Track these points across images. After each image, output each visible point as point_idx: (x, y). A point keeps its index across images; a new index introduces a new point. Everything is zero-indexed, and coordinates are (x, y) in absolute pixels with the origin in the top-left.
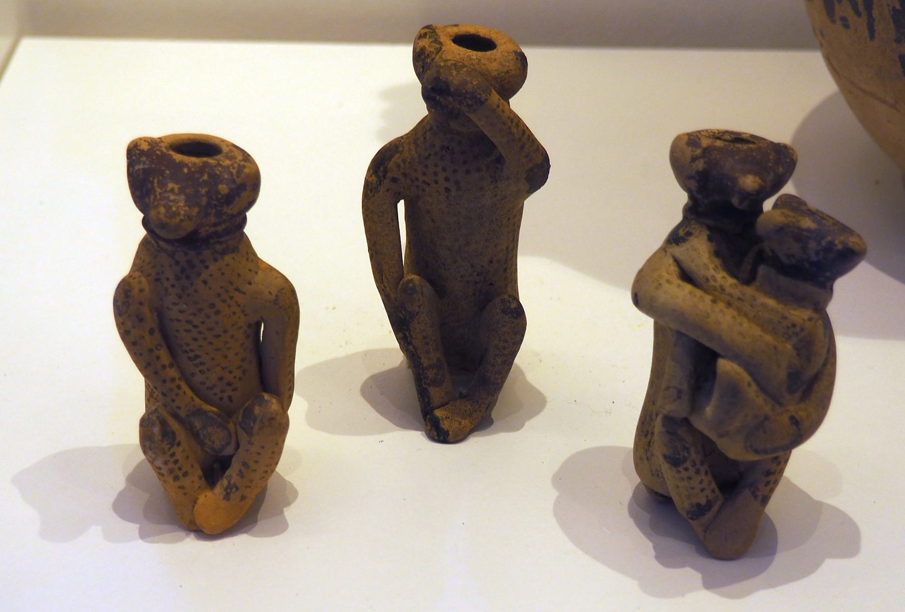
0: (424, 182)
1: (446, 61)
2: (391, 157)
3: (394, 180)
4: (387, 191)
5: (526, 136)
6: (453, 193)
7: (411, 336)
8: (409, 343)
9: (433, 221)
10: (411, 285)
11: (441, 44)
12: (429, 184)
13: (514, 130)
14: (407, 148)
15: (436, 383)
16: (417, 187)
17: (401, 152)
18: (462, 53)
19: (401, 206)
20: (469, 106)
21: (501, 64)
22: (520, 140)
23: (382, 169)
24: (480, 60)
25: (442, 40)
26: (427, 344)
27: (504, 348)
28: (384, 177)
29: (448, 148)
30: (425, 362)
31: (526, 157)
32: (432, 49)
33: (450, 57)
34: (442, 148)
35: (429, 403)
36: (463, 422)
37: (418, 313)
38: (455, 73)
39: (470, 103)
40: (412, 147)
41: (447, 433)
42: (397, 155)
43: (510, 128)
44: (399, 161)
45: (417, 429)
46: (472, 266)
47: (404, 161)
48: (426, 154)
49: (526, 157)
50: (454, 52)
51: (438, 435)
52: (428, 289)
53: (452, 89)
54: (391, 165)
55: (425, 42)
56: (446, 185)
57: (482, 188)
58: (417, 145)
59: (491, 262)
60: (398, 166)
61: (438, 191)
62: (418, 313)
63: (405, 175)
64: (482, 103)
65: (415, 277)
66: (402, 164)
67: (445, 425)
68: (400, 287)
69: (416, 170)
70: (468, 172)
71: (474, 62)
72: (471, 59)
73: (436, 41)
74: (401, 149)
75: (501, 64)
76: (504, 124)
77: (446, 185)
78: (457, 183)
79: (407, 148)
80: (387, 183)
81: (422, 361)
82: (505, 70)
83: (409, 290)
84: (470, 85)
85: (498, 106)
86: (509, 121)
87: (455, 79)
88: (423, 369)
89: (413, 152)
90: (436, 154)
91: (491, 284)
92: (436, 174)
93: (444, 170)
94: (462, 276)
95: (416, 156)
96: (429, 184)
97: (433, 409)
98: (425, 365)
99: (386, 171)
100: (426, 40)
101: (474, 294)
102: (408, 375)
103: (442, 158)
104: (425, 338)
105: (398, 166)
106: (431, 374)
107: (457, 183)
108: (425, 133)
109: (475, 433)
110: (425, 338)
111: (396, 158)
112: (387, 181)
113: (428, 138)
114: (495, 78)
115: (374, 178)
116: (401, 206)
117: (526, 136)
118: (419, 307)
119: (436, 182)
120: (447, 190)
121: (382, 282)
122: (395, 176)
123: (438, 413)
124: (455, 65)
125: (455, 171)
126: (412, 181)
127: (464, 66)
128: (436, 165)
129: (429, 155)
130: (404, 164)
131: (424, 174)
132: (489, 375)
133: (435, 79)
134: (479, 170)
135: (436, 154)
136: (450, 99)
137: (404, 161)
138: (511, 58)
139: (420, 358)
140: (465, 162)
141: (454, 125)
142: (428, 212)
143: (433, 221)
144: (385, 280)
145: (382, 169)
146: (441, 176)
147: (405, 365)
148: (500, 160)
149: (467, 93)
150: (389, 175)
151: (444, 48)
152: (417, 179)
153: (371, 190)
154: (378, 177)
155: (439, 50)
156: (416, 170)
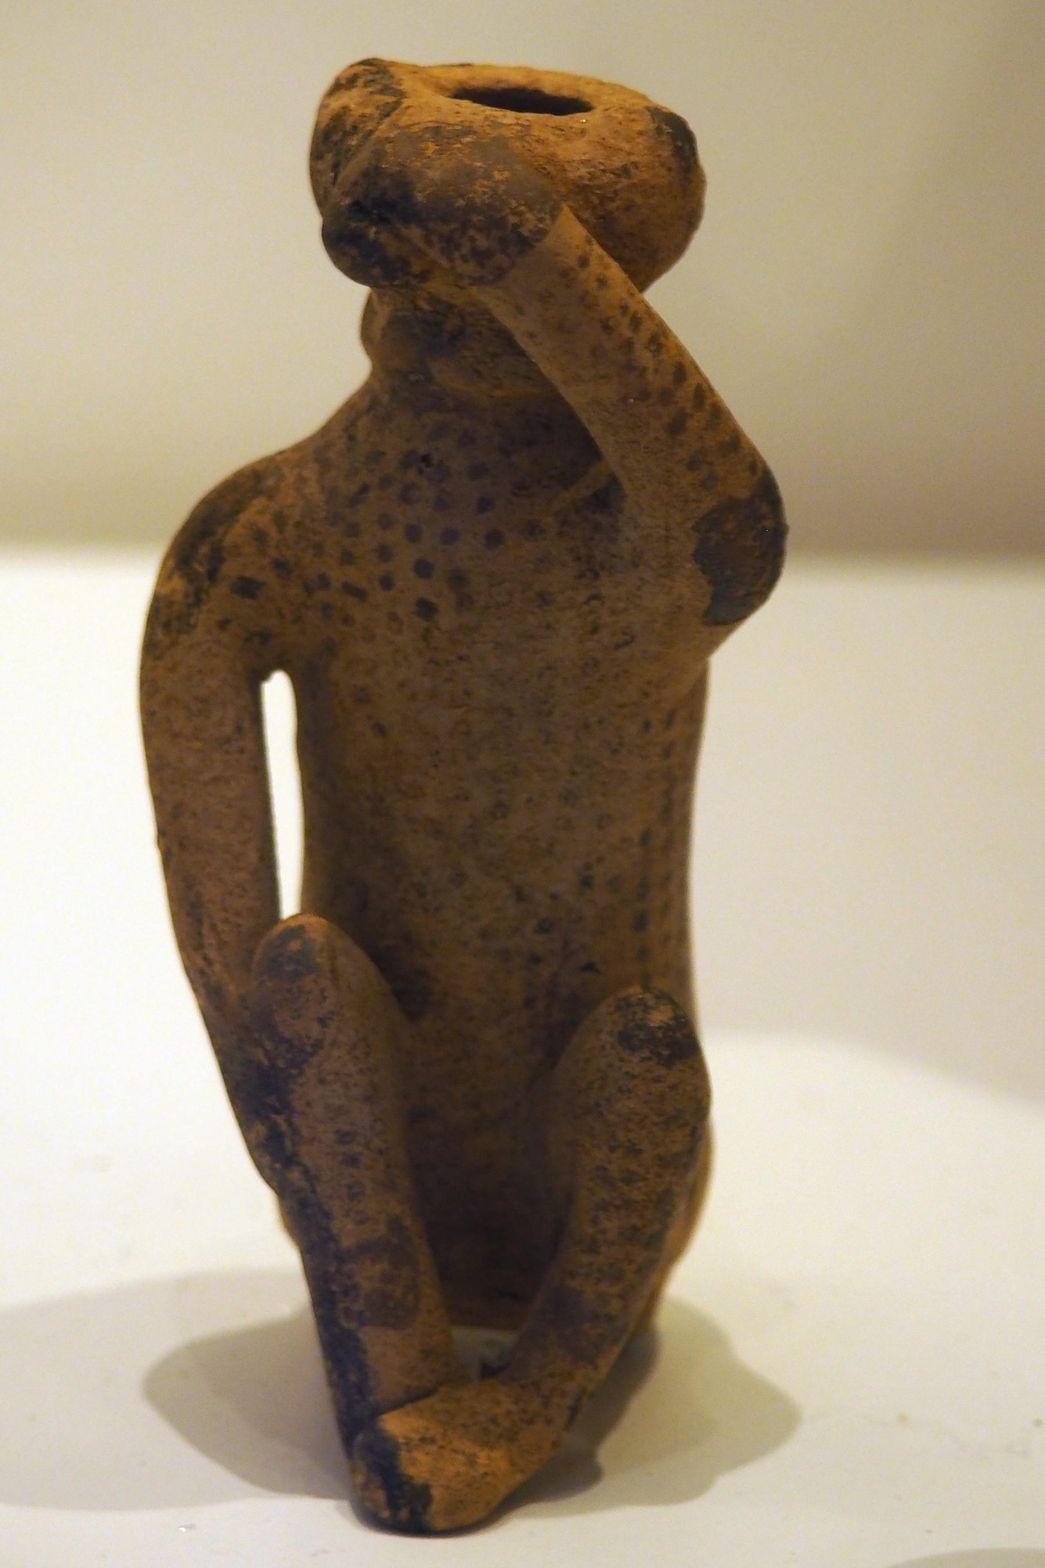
0: (349, 589)
2: (239, 507)
3: (247, 588)
4: (223, 625)
6: (447, 619)
7: (295, 1132)
9: (381, 730)
10: (295, 946)
12: (360, 594)
13: (645, 357)
14: (290, 476)
15: (390, 1312)
16: (327, 609)
17: (271, 494)
19: (278, 695)
20: (481, 256)
22: (666, 397)
23: (204, 549)
26: (353, 1161)
27: (629, 1178)
28: (212, 575)
29: (426, 459)
30: (348, 1232)
31: (693, 465)
34: (408, 460)
35: (362, 1389)
36: (483, 1456)
37: (318, 1045)
39: (482, 243)
40: (310, 472)
41: (422, 1495)
42: (259, 503)
43: (628, 346)
44: (264, 522)
46: (520, 896)
48: (354, 488)
49: (693, 465)
51: (393, 1503)
52: (356, 965)
53: (420, 197)
54: (236, 534)
56: (423, 589)
59: (586, 883)
60: (260, 537)
61: (393, 617)
62: (318, 1045)
63: (280, 565)
64: (524, 244)
66: (273, 533)
67: (417, 1466)
69: (318, 549)
70: (494, 539)
76: (607, 328)
77: (423, 589)
78: (458, 580)
79: (290, 476)
80: (220, 599)
81: (336, 1226)
82: (618, 162)
86: (626, 321)
88: (341, 1258)
89: (312, 489)
92: (384, 553)
94: (484, 934)
96: (360, 594)
97: (377, 1412)
98: (347, 1242)
99: (217, 558)
101: (529, 1003)
103: (405, 497)
104: (344, 1137)
106: (367, 1276)
107: (458, 580)
109: (532, 1508)
110: (344, 1137)
112: (220, 591)
115: (178, 583)
116: (278, 695)
118: (323, 1022)
119: (387, 583)
120: (426, 609)
121: (199, 947)
122: (248, 574)
123: (395, 1425)
125: (450, 536)
126: (308, 589)
129: (365, 489)
132: (575, 1284)
134: (532, 529)
135: (385, 482)
136: (414, 233)
137: (280, 520)
138: (638, 127)
139: (327, 1215)
140: (484, 505)
141: (446, 375)
142: (363, 697)
143: (381, 730)
144: (210, 940)
145: (204, 549)
146: (406, 556)
148: (606, 499)
149: (471, 207)
150: (230, 569)
152: (324, 582)
153: (167, 625)
154: (190, 577)
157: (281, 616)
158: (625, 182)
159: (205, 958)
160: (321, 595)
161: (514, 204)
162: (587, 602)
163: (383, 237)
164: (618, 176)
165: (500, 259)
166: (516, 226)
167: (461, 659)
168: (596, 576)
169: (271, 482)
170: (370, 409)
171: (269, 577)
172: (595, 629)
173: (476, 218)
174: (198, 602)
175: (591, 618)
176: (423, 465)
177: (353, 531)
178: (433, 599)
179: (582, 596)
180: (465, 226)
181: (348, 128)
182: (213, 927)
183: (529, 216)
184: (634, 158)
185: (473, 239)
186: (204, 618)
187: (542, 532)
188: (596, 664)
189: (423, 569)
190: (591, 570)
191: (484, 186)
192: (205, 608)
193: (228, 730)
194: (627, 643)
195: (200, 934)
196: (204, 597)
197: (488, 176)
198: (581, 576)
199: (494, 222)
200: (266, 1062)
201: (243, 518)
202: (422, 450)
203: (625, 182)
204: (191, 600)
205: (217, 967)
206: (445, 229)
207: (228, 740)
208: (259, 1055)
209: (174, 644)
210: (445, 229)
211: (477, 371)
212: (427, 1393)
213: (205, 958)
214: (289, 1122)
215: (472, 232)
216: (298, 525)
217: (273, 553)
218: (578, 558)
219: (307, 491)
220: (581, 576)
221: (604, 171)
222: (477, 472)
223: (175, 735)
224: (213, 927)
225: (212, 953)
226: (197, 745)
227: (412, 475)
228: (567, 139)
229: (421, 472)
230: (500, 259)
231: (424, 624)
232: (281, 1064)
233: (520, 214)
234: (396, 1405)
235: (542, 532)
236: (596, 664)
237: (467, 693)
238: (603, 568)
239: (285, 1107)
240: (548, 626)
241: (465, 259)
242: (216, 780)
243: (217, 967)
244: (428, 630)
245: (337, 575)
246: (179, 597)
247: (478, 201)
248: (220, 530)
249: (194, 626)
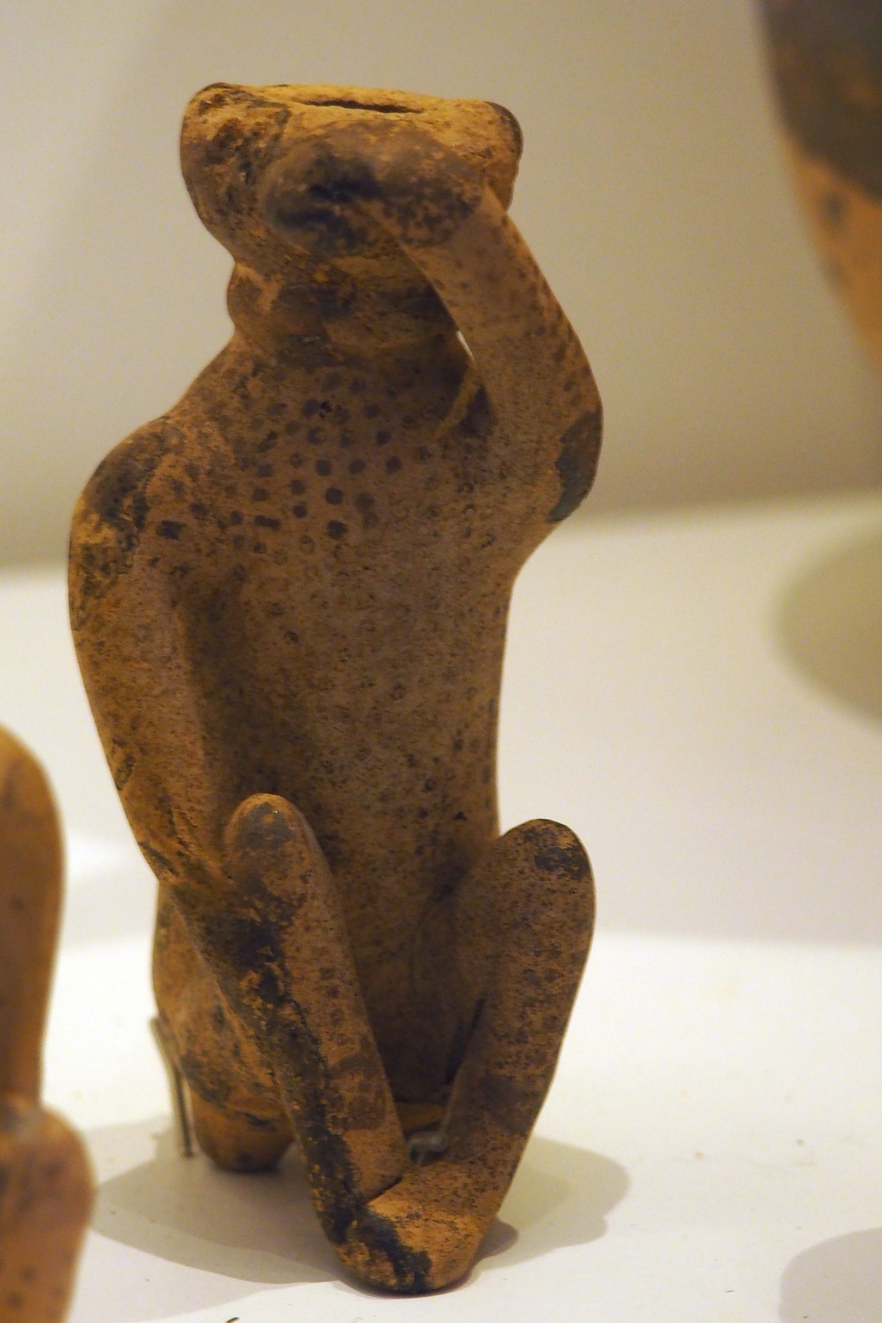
0: (261, 521)
2: (151, 465)
3: (169, 530)
4: (153, 562)
6: (355, 536)
7: (287, 974)
9: (293, 637)
10: (268, 820)
12: (274, 524)
15: (365, 1117)
16: (238, 541)
17: (179, 450)
20: (431, 222)
23: (128, 502)
26: (333, 993)
28: (140, 522)
29: (325, 406)
34: (309, 408)
35: (347, 1184)
36: (459, 1222)
37: (302, 899)
39: (434, 210)
40: (210, 428)
41: (422, 1261)
42: (169, 459)
46: (412, 762)
47: (192, 471)
48: (261, 435)
49: (568, 387)
51: (399, 1272)
56: (334, 513)
57: (433, 512)
58: (223, 422)
59: (458, 746)
60: (177, 487)
62: (302, 899)
63: (198, 509)
66: (187, 481)
67: (413, 1238)
68: (230, 833)
69: (231, 491)
70: (393, 465)
75: (466, 131)
77: (334, 513)
78: (365, 502)
79: (192, 435)
80: (148, 542)
81: (323, 1050)
82: (482, 146)
88: (328, 1076)
89: (217, 441)
90: (291, 428)
91: (460, 816)
92: (298, 487)
93: (323, 468)
94: (383, 798)
95: (225, 449)
96: (274, 524)
98: (332, 1062)
99: (141, 508)
101: (419, 851)
103: (313, 437)
104: (327, 973)
106: (349, 1088)
107: (365, 502)
108: (242, 384)
109: (484, 1262)
110: (327, 973)
111: (166, 466)
112: (149, 533)
118: (303, 878)
119: (300, 512)
120: (337, 530)
122: (171, 518)
123: (384, 1208)
125: (357, 467)
126: (222, 526)
128: (297, 461)
129: (273, 435)
132: (506, 1071)
134: (422, 455)
136: (375, 208)
137: (192, 471)
138: (487, 118)
139: (316, 1041)
140: (383, 438)
141: (342, 335)
142: (276, 611)
143: (293, 637)
144: (180, 826)
145: (128, 502)
146: (318, 486)
149: (422, 182)
150: (154, 516)
152: (237, 518)
153: (105, 569)
154: (120, 526)
156: (231, 491)
157: (199, 551)
158: (489, 162)
159: (181, 842)
160: (234, 530)
161: (454, 177)
162: (464, 512)
163: (348, 213)
164: (484, 157)
165: (448, 223)
166: (459, 196)
167: (366, 568)
168: (471, 489)
169: (174, 441)
170: (255, 374)
171: (188, 519)
172: (468, 534)
173: (428, 191)
174: (131, 546)
175: (467, 524)
176: (323, 411)
177: (266, 471)
178: (343, 521)
179: (460, 507)
180: (420, 197)
181: (248, 134)
182: (182, 815)
183: (467, 187)
184: (492, 143)
185: (426, 208)
186: (137, 559)
187: (430, 455)
188: (468, 561)
189: (334, 496)
190: (467, 484)
191: (429, 165)
192: (137, 550)
193: (167, 650)
194: (489, 543)
195: (171, 822)
196: (135, 541)
197: (429, 156)
198: (460, 490)
199: (442, 193)
200: (258, 919)
201: (158, 472)
202: (320, 399)
203: (489, 162)
204: (124, 545)
205: (193, 848)
206: (404, 201)
207: (169, 659)
208: (253, 914)
209: (114, 583)
210: (404, 201)
211: (369, 329)
212: (398, 1180)
213: (181, 842)
214: (282, 967)
215: (426, 203)
216: (209, 473)
217: (190, 498)
218: (457, 476)
219: (212, 445)
220: (460, 490)
221: (473, 154)
222: (372, 411)
223: (126, 660)
224: (182, 815)
225: (186, 838)
226: (146, 665)
227: (315, 420)
228: (439, 130)
229: (322, 416)
230: (448, 223)
231: (334, 543)
232: (272, 918)
233: (460, 185)
234: (378, 1194)
235: (430, 455)
236: (468, 561)
237: (372, 597)
238: (476, 482)
239: (278, 955)
240: (436, 534)
241: (418, 225)
242: (165, 692)
243: (193, 848)
244: (338, 547)
245: (249, 511)
246: (112, 544)
247: (427, 177)
248: (140, 485)
249: (131, 566)
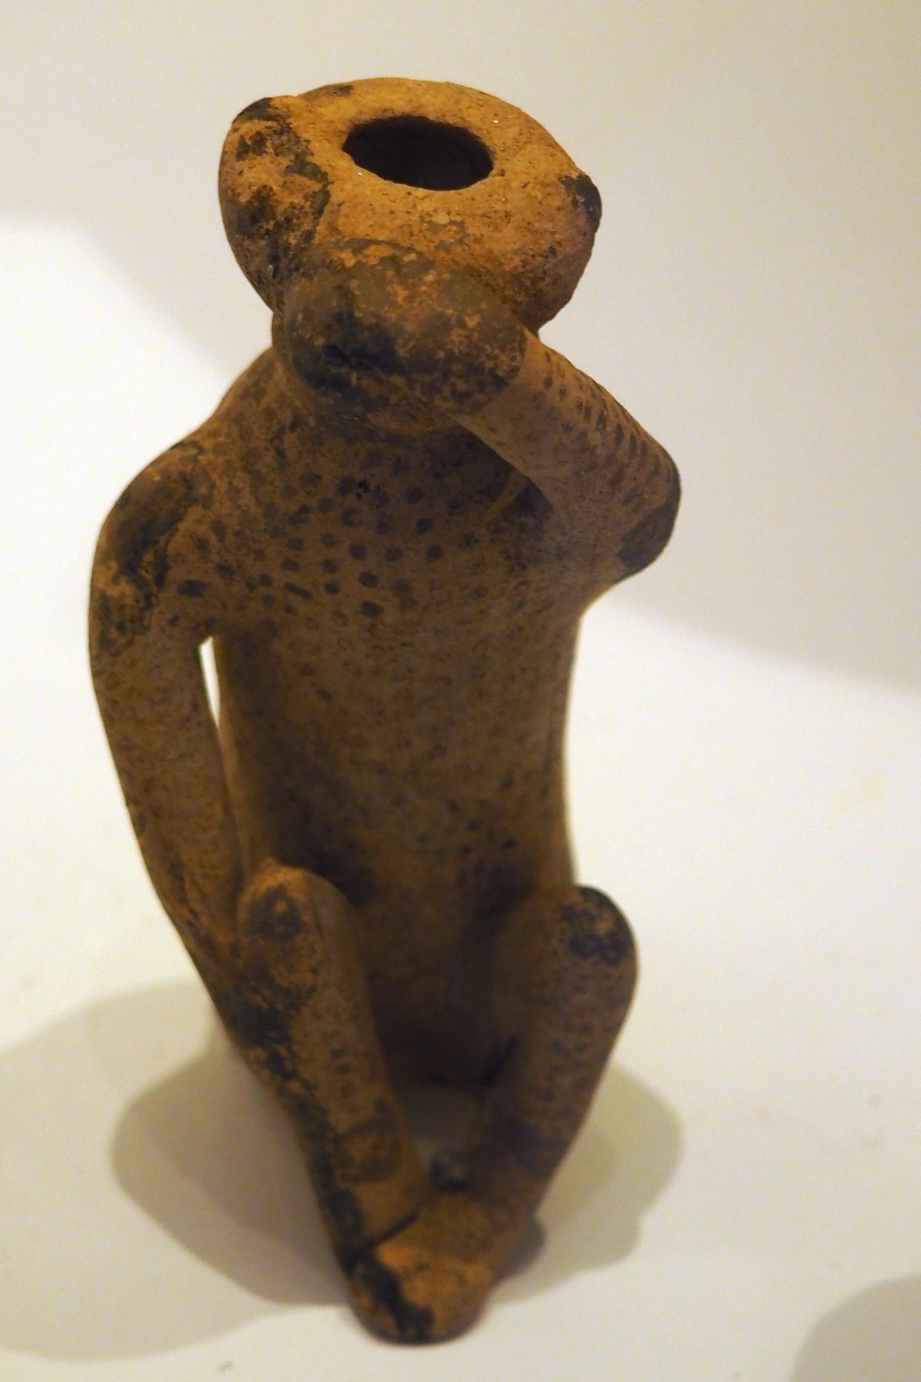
0: (290, 588)
1: (360, 245)
2: (176, 518)
3: (192, 589)
4: (174, 622)
5: (626, 444)
6: (390, 616)
8: (289, 1076)
9: (325, 695)
10: (280, 907)
11: (318, 174)
12: (306, 595)
13: (595, 438)
14: (222, 485)
16: (268, 601)
17: (207, 502)
18: (399, 207)
20: (460, 397)
21: (528, 227)
22: (610, 459)
23: (148, 557)
24: (461, 225)
25: (317, 160)
27: (581, 1048)
28: (160, 581)
29: (363, 485)
30: (341, 1121)
31: (627, 501)
32: (298, 199)
33: (362, 229)
34: (345, 486)
37: (312, 990)
38: (401, 294)
39: (462, 386)
40: (242, 481)
42: (195, 512)
43: (584, 434)
44: (203, 530)
45: (320, 1299)
46: (454, 807)
47: (219, 529)
48: (293, 507)
50: (372, 202)
51: (401, 1325)
53: (402, 352)
54: (178, 542)
55: (263, 172)
56: (369, 595)
57: (479, 594)
58: (257, 479)
59: (507, 785)
60: (202, 545)
61: (338, 614)
62: (312, 990)
63: (224, 569)
64: (500, 383)
65: (289, 877)
66: (214, 540)
67: (417, 1292)
68: (242, 915)
69: (260, 555)
70: (435, 553)
71: (448, 237)
72: (435, 228)
73: (302, 165)
74: (203, 490)
75: (528, 227)
76: (567, 428)
78: (402, 588)
79: (222, 485)
80: (169, 600)
82: (545, 246)
83: (277, 924)
84: (456, 337)
85: (548, 383)
86: (581, 417)
87: (405, 310)
89: (247, 499)
90: (325, 506)
91: (509, 844)
92: (329, 566)
93: (358, 552)
95: (257, 511)
96: (306, 595)
97: (373, 1244)
99: (162, 566)
100: (266, 159)
102: (236, 1078)
103: (348, 519)
104: (336, 1054)
105: (202, 545)
107: (402, 588)
108: (279, 435)
110: (336, 1054)
111: (193, 521)
113: (291, 454)
114: (516, 278)
115: (125, 590)
117: (626, 444)
118: (314, 971)
119: (332, 589)
120: (370, 609)
121: (184, 901)
122: (193, 577)
123: (392, 1256)
124: (393, 261)
125: (393, 555)
126: (250, 586)
127: (427, 265)
128: (329, 541)
129: (305, 509)
130: (221, 538)
131: (290, 565)
133: (338, 318)
134: (468, 541)
135: (325, 506)
136: (398, 380)
137: (219, 529)
138: (556, 202)
140: (424, 526)
142: (307, 670)
143: (325, 695)
144: (192, 894)
147: (223, 1044)
148: (529, 501)
150: (176, 575)
151: (336, 196)
152: (266, 580)
153: (121, 627)
154: (138, 582)
155: (321, 202)
156: (260, 555)
157: (224, 606)
158: (552, 261)
159: (192, 911)
160: (264, 590)
161: (488, 348)
162: (516, 589)
163: (365, 383)
164: (546, 257)
165: (478, 397)
166: (492, 371)
167: (404, 645)
168: (524, 568)
169: (203, 490)
170: (294, 427)
171: (214, 579)
172: (521, 605)
173: (455, 367)
174: (149, 606)
175: (519, 599)
176: (361, 491)
177: (297, 545)
178: (377, 601)
179: (513, 584)
180: (446, 375)
181: (281, 218)
182: (194, 883)
183: (503, 358)
184: (558, 237)
185: (453, 385)
186: (156, 619)
187: (477, 541)
188: (521, 629)
189: (368, 580)
190: (518, 563)
191: (460, 336)
192: (156, 611)
193: (187, 710)
194: (546, 608)
195: (183, 889)
196: (153, 600)
197: (462, 324)
198: (512, 569)
199: (473, 369)
200: (265, 1006)
201: (182, 526)
202: (359, 477)
203: (552, 261)
204: (142, 604)
205: (204, 919)
206: (428, 379)
207: (188, 719)
208: (258, 1000)
209: (130, 643)
210: (428, 379)
211: (413, 417)
212: (411, 1219)
213: (192, 911)
214: (289, 1049)
215: (453, 379)
216: (237, 534)
217: (215, 558)
218: (509, 558)
219: (242, 502)
220: (512, 569)
221: (533, 256)
222: (414, 496)
223: (140, 722)
224: (194, 883)
225: (198, 907)
226: (162, 728)
227: (351, 500)
228: (497, 228)
229: (359, 496)
230: (478, 397)
231: (368, 621)
232: (280, 1007)
233: (496, 357)
234: (389, 1235)
235: (477, 541)
236: (521, 629)
237: (410, 670)
238: (529, 562)
239: (286, 1039)
240: (482, 612)
241: (445, 399)
242: (182, 756)
243: (204, 919)
244: (373, 626)
245: (280, 577)
246: (129, 601)
247: (456, 351)
248: (162, 540)
249: (149, 628)
